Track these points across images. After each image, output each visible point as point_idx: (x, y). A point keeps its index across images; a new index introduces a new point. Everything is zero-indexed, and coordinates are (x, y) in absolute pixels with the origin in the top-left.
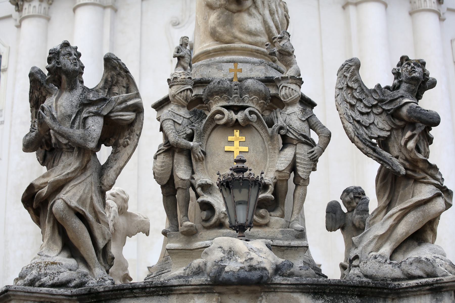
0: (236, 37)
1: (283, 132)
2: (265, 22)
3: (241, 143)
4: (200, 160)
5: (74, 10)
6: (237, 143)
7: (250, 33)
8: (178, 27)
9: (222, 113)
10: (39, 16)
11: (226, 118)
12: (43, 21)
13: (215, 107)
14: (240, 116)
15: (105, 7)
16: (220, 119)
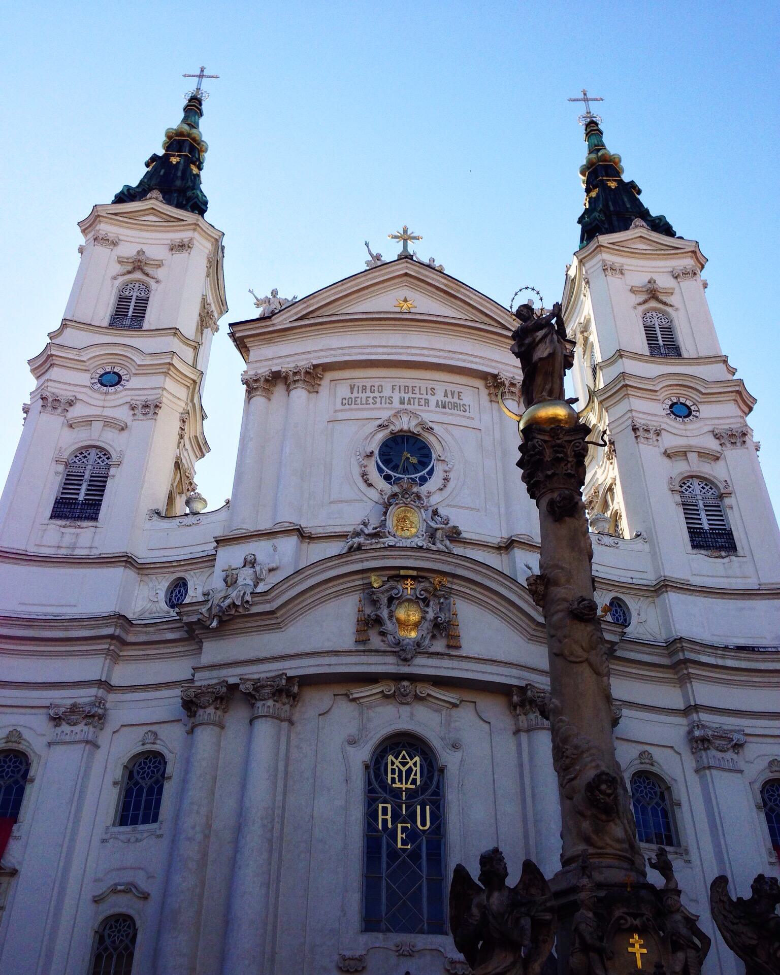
0: (607, 844)
1: (674, 938)
2: (626, 831)
3: (641, 946)
4: (609, 959)
5: (251, 722)
6: (637, 946)
7: (618, 841)
8: (354, 745)
9: (626, 920)
10: (214, 725)
11: (629, 924)
12: (217, 729)
13: (618, 913)
14: (637, 922)
15: (282, 721)
16: (624, 924)
